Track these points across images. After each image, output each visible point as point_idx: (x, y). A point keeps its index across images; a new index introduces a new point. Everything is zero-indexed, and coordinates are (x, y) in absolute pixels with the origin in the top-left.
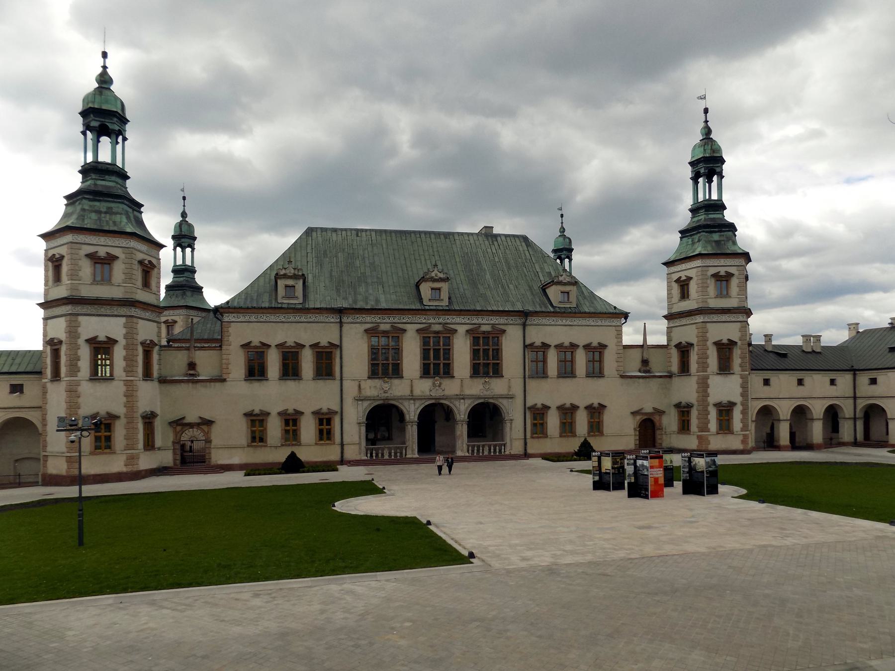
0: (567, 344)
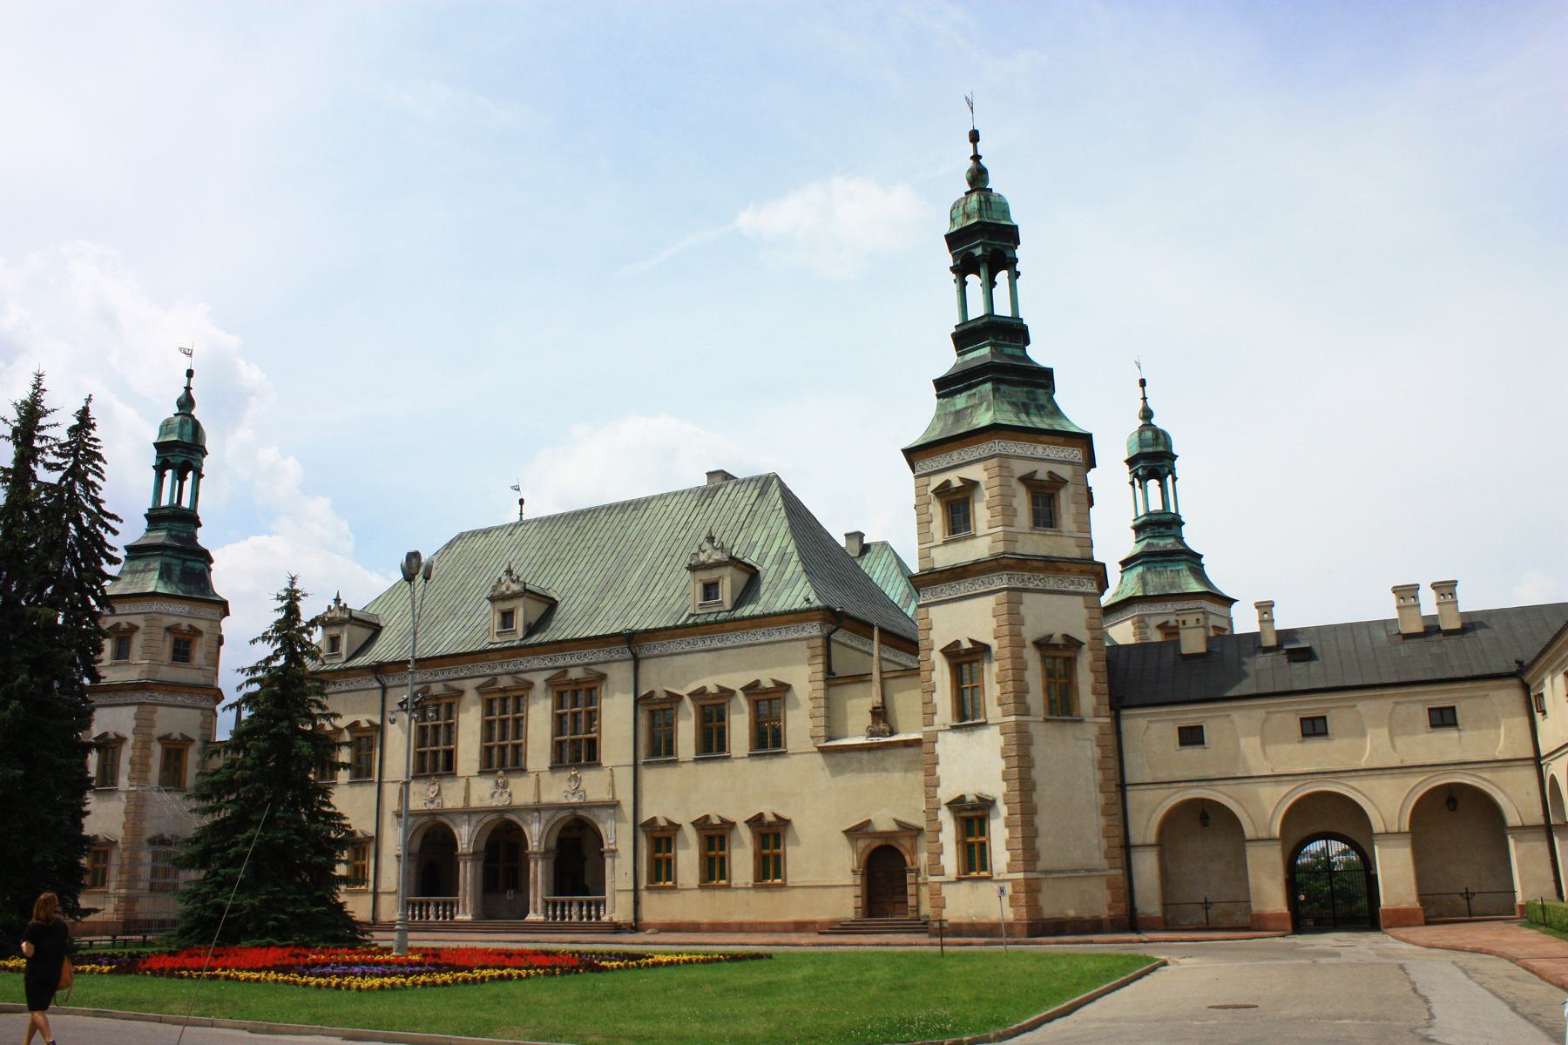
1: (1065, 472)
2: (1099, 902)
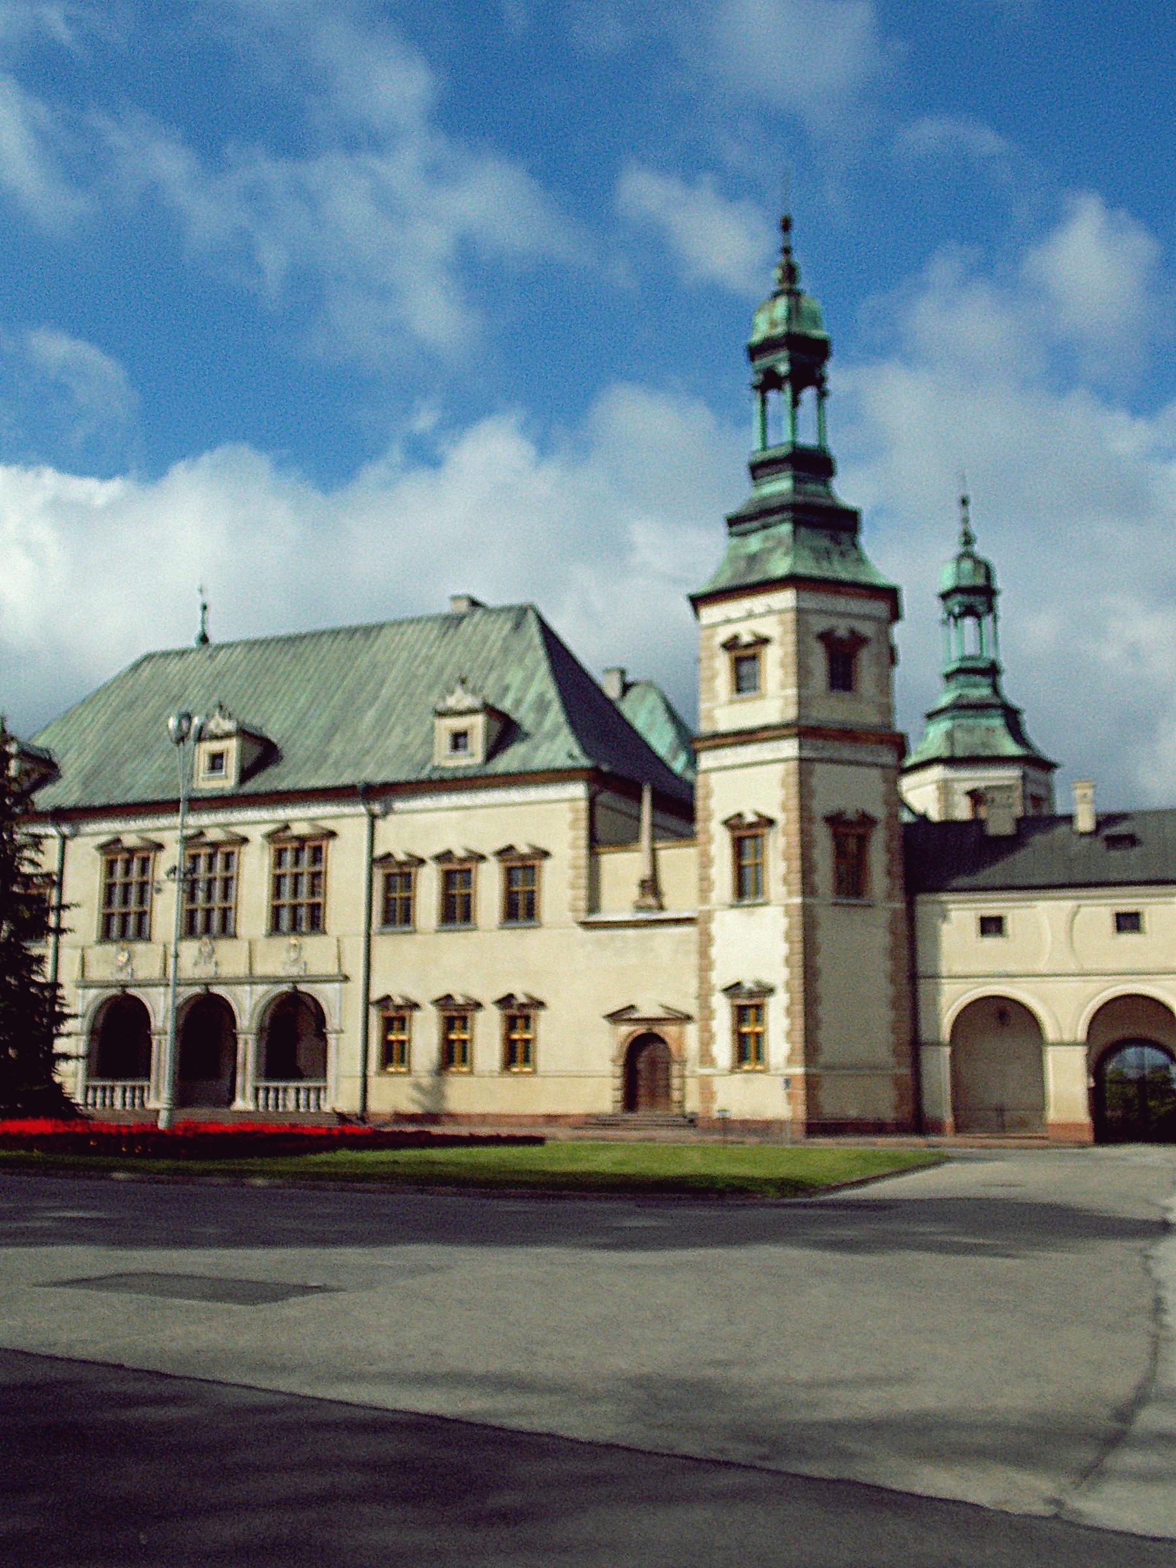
0: (460, 853)
1: (867, 629)
2: (883, 1102)
